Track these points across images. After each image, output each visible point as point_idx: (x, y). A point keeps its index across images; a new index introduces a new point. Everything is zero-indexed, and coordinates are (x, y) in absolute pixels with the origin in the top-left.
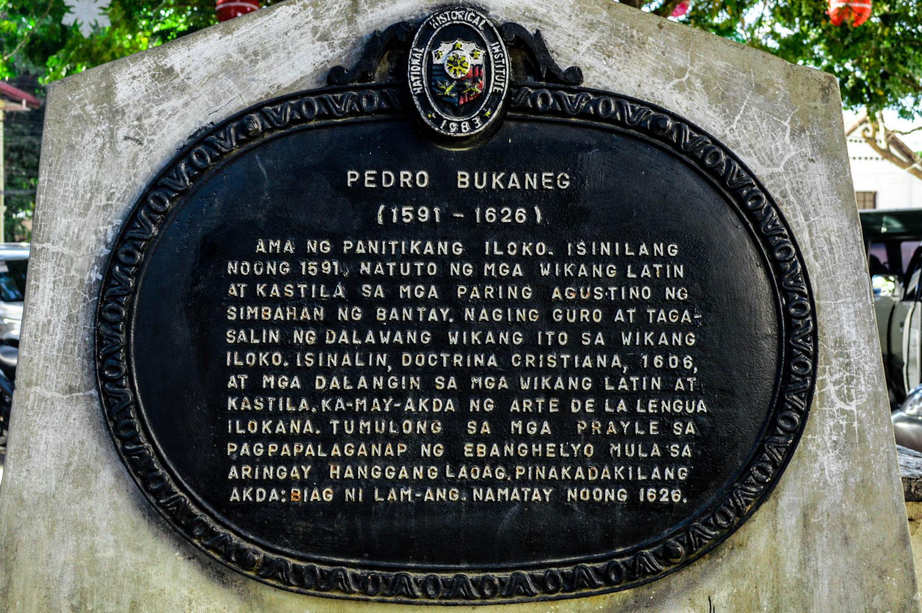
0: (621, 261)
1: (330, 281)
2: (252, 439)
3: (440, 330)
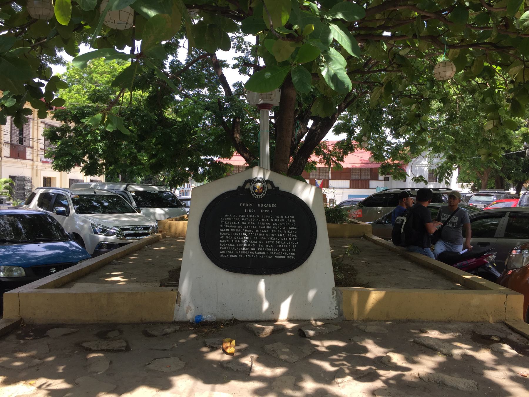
0: (285, 219)
1: (237, 222)
2: (224, 247)
3: (255, 230)
